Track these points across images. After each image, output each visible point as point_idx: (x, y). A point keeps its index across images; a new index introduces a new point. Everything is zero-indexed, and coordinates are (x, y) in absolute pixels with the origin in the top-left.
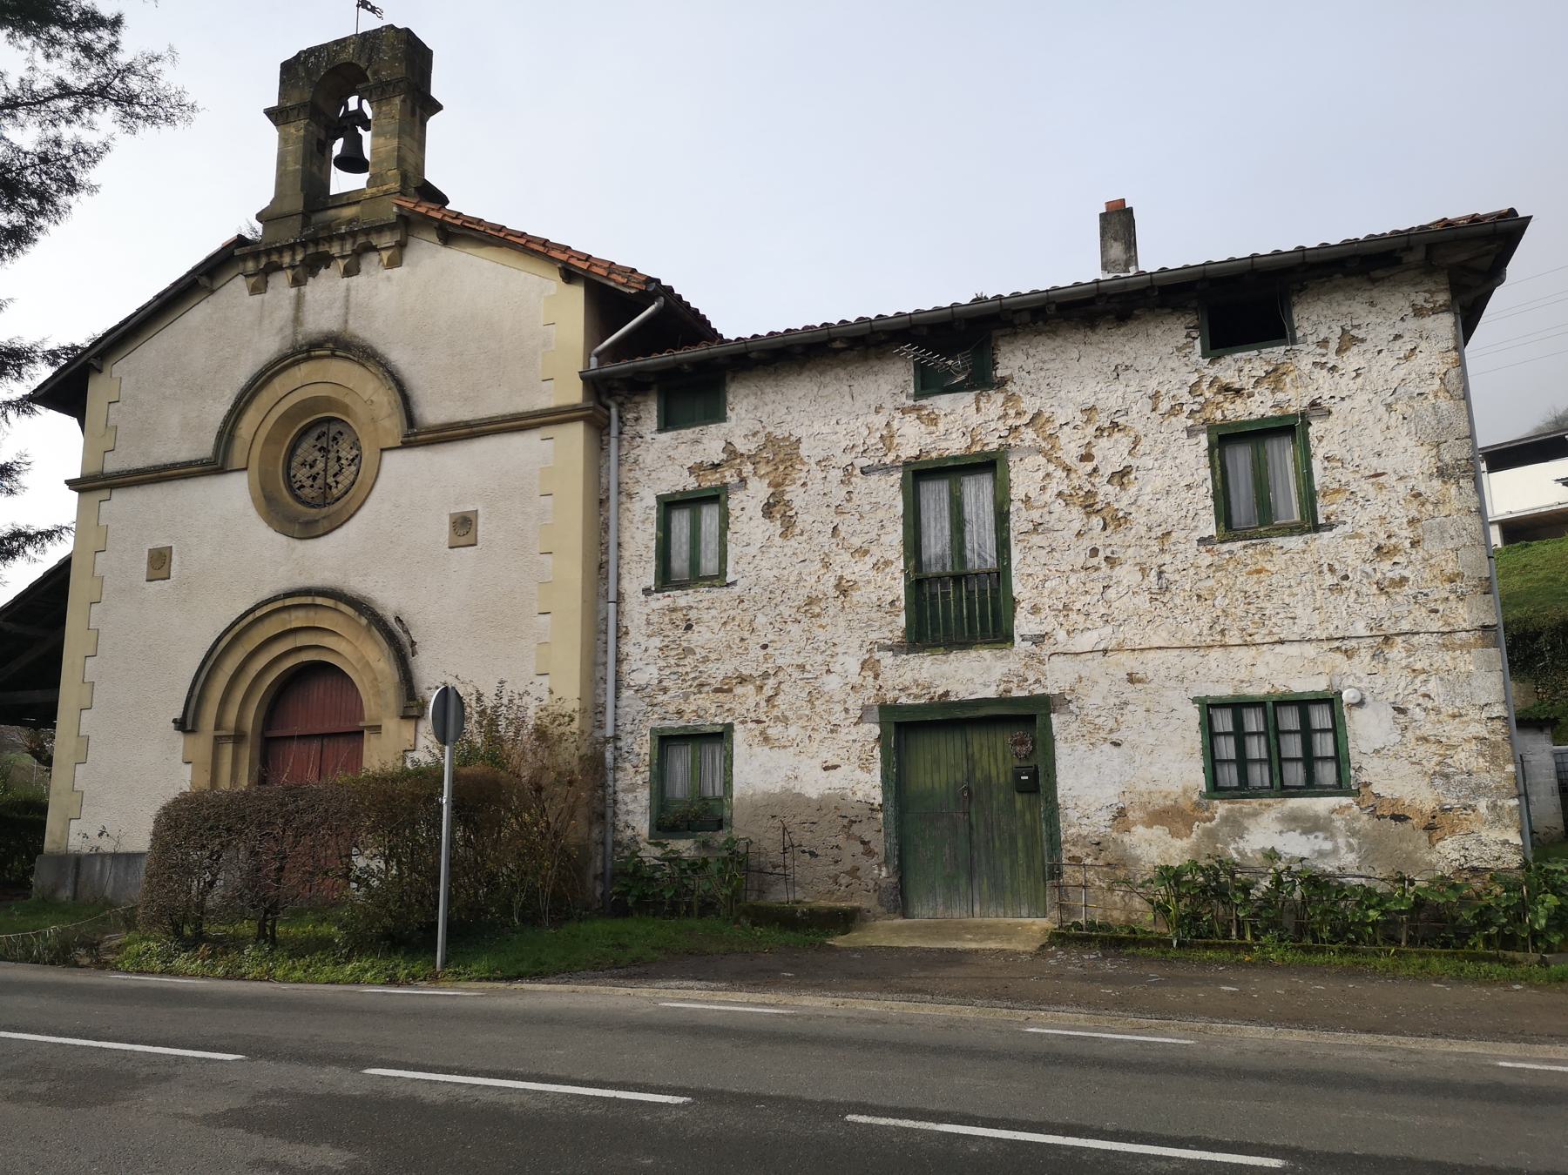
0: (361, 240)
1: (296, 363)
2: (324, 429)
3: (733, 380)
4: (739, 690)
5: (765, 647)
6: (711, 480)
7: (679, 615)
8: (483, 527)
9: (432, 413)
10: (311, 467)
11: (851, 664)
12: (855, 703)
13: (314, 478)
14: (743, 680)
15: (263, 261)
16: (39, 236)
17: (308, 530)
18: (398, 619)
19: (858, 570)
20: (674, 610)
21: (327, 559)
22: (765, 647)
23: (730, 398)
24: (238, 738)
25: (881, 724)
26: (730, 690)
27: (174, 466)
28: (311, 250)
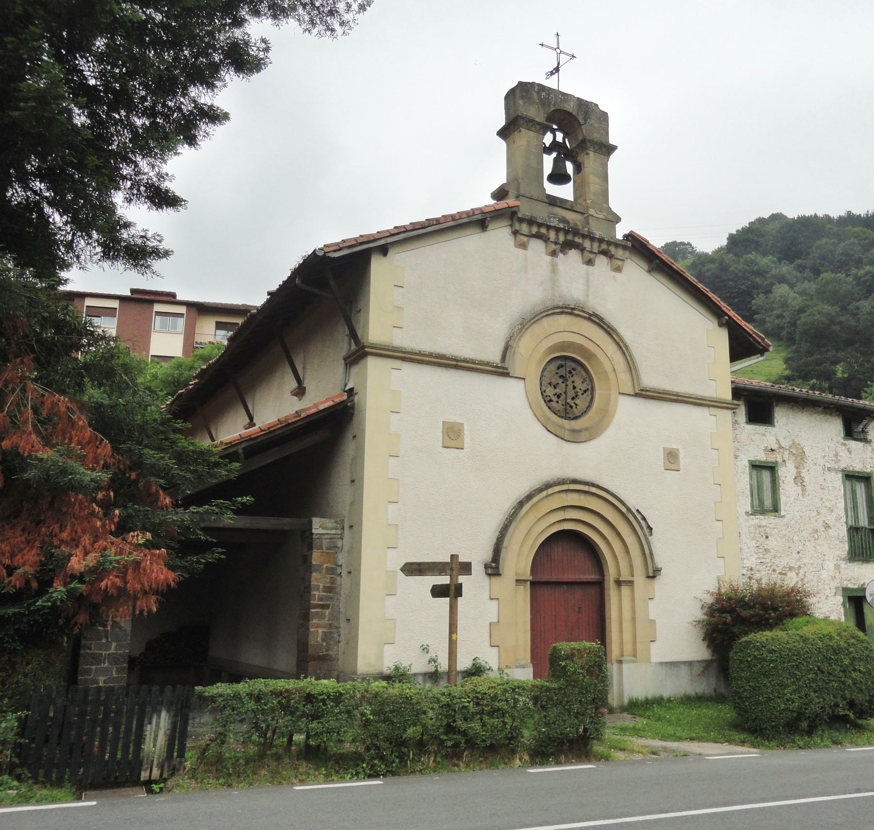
0: (604, 246)
1: (562, 313)
2: (563, 363)
3: (777, 405)
4: (789, 574)
5: (799, 553)
6: (770, 458)
7: (762, 529)
8: (683, 460)
9: (650, 380)
10: (555, 387)
11: (830, 565)
12: (834, 584)
13: (559, 397)
14: (791, 569)
15: (534, 230)
16: (229, 92)
17: (575, 437)
18: (638, 510)
19: (831, 519)
20: (760, 527)
21: (584, 460)
22: (799, 553)
23: (776, 415)
24: (619, 583)
25: (843, 596)
26: (785, 574)
27: (420, 354)
28: (570, 237)
